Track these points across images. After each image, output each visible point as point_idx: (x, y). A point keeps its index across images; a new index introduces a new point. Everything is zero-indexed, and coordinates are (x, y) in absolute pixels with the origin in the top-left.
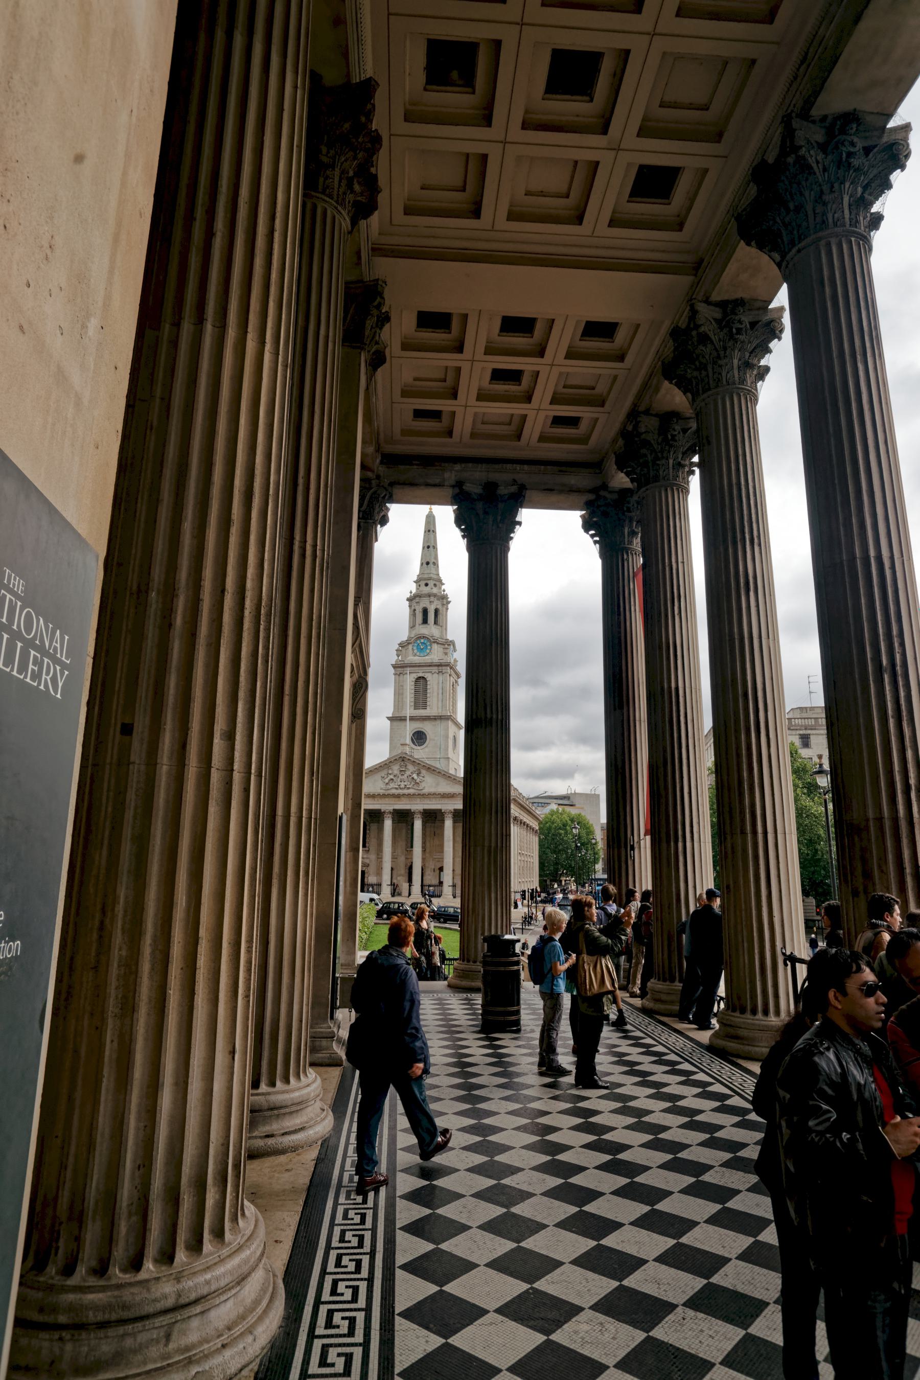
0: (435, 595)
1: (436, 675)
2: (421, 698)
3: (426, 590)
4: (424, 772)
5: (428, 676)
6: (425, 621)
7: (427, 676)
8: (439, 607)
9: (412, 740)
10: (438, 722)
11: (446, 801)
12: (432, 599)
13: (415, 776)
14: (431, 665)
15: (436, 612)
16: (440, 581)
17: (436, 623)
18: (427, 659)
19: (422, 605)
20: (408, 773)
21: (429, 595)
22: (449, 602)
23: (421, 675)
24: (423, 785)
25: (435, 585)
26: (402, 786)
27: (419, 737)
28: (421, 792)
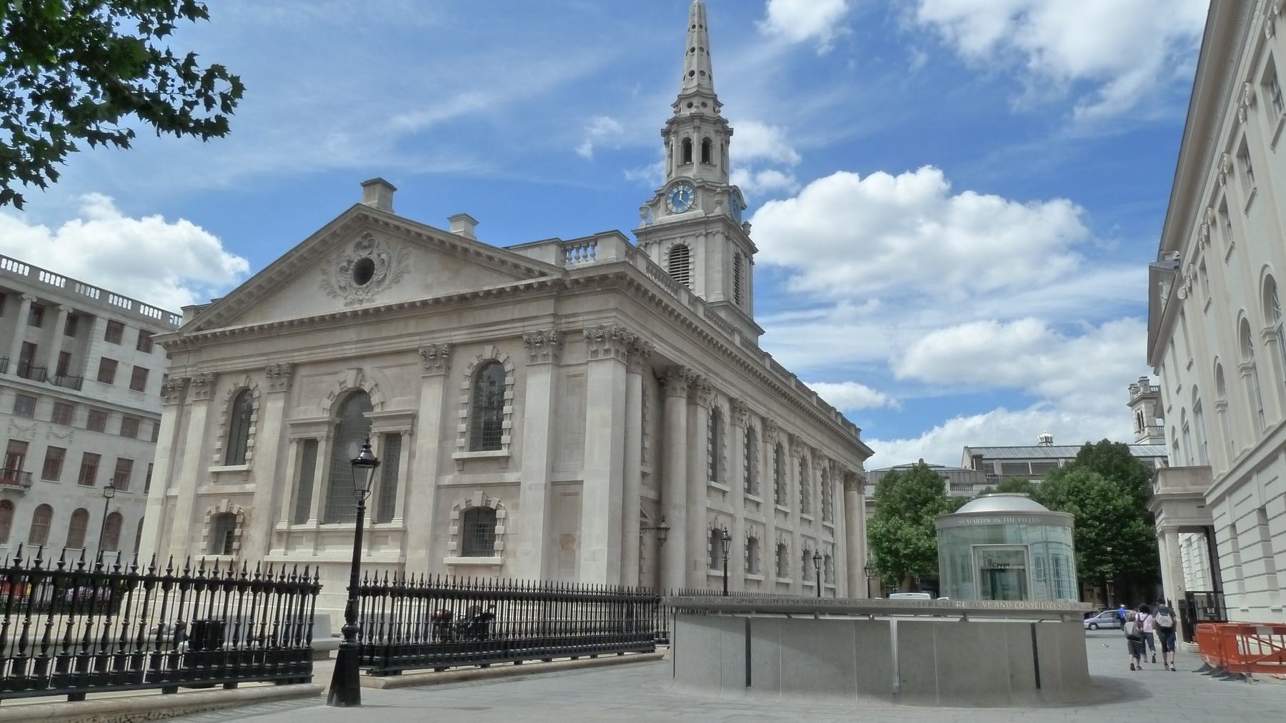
0: (702, 118)
1: (702, 239)
3: (686, 112)
5: (690, 242)
7: (688, 242)
8: (712, 135)
12: (697, 122)
14: (696, 223)
15: (706, 146)
16: (714, 98)
17: (706, 157)
19: (683, 135)
21: (693, 117)
22: (730, 132)
23: (678, 241)
25: (704, 105)
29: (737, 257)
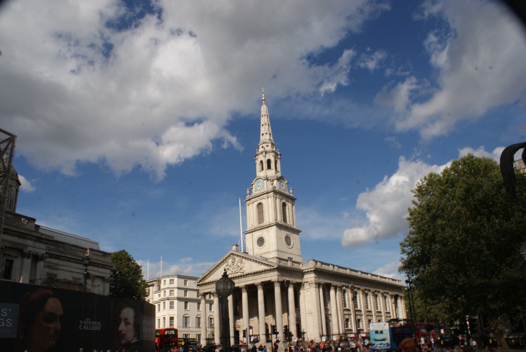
0: (266, 152)
1: (267, 199)
2: (261, 218)
4: (244, 260)
5: (264, 202)
6: (262, 169)
9: (258, 244)
10: (270, 228)
11: (256, 277)
13: (239, 264)
15: (269, 162)
17: (269, 167)
18: (262, 191)
20: (236, 262)
23: (259, 202)
24: (244, 269)
25: (267, 146)
26: (234, 272)
27: (261, 241)
28: (242, 274)
29: (284, 205)
